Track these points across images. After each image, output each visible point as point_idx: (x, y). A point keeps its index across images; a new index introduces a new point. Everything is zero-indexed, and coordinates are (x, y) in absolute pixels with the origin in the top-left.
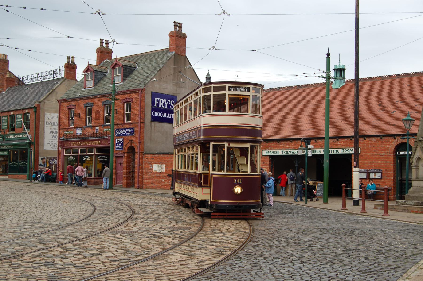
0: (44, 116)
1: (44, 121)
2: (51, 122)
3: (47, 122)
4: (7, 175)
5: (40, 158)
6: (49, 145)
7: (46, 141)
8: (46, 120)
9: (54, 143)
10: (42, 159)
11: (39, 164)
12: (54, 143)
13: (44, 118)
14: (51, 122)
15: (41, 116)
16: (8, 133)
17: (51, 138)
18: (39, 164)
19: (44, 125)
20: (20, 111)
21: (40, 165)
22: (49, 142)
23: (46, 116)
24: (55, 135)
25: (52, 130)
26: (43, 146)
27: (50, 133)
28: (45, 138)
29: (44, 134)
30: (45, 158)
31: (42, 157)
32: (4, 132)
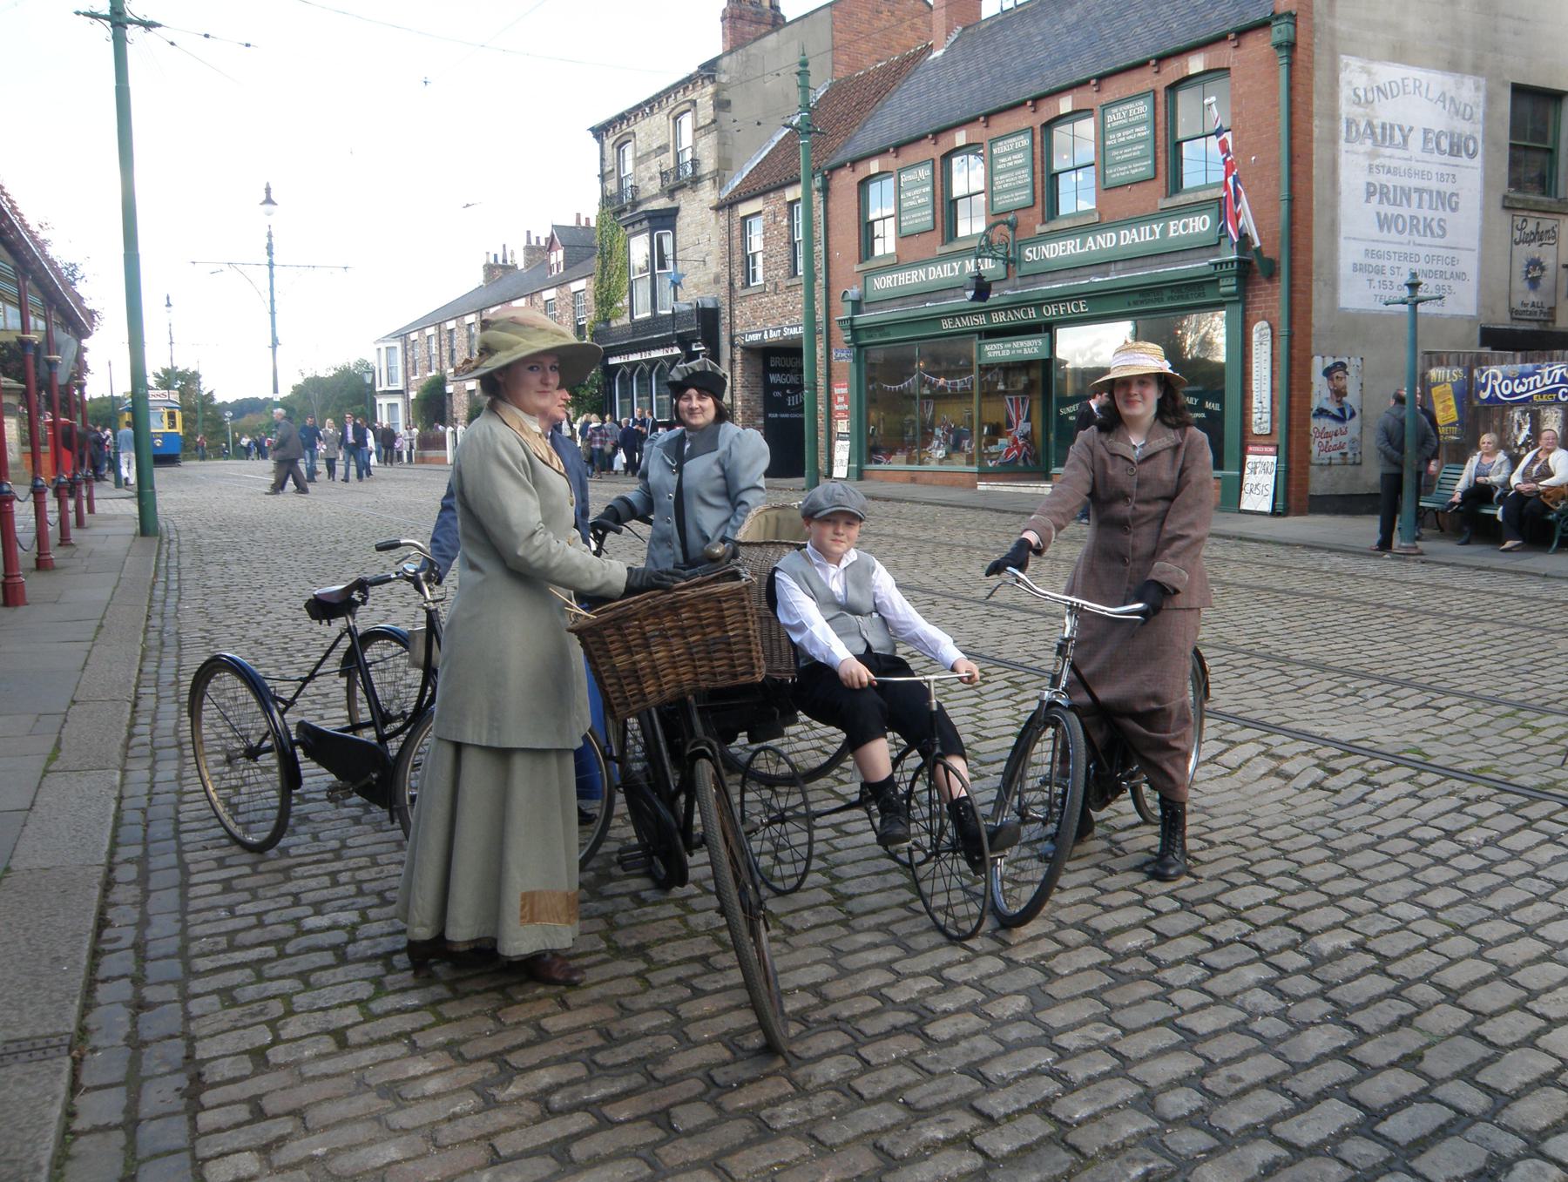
0: (1335, 81)
1: (1333, 116)
2: (1370, 124)
3: (1350, 123)
4: (1047, 477)
5: (1318, 364)
6: (1362, 278)
7: (1349, 253)
8: (1346, 109)
9: (1388, 264)
10: (1328, 372)
11: (1315, 404)
12: (1388, 264)
13: (1334, 95)
14: (1370, 124)
15: (1320, 77)
16: (1039, 229)
17: (1374, 231)
18: (1315, 404)
19: (1333, 140)
20: (1136, 76)
21: (1322, 412)
22: (1360, 259)
23: (1344, 76)
24: (1395, 210)
25: (1382, 178)
26: (1333, 284)
27: (1370, 194)
28: (1345, 229)
29: (1333, 206)
30: (1343, 366)
31: (1329, 362)
32: (1013, 226)
